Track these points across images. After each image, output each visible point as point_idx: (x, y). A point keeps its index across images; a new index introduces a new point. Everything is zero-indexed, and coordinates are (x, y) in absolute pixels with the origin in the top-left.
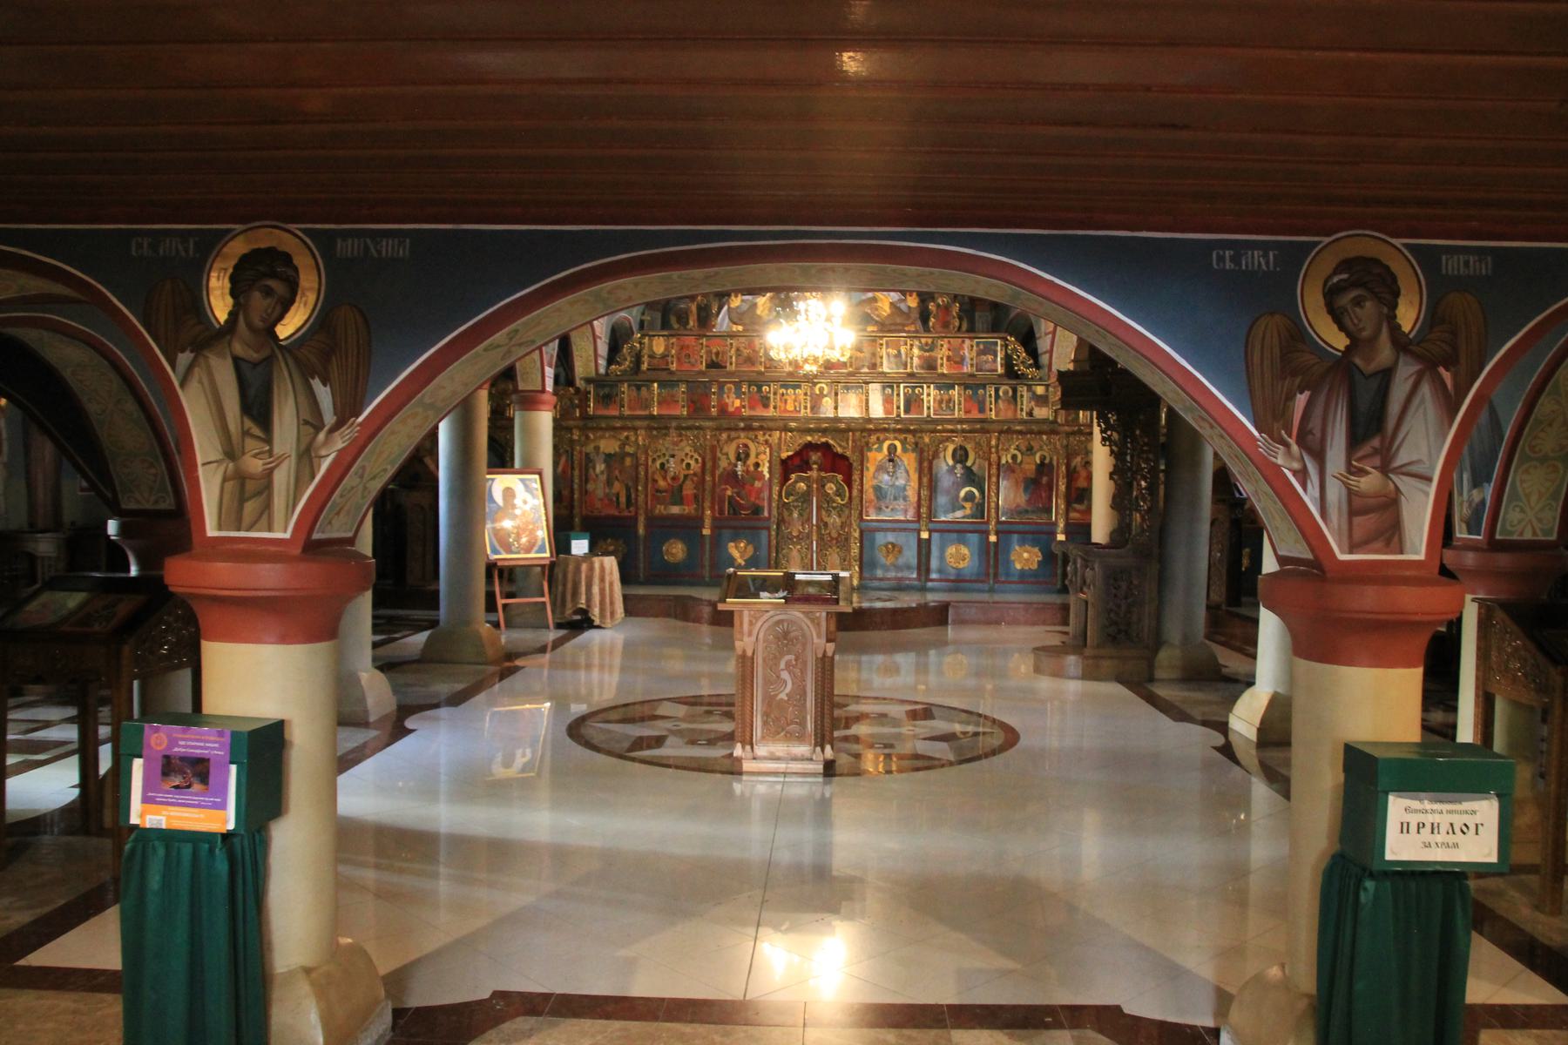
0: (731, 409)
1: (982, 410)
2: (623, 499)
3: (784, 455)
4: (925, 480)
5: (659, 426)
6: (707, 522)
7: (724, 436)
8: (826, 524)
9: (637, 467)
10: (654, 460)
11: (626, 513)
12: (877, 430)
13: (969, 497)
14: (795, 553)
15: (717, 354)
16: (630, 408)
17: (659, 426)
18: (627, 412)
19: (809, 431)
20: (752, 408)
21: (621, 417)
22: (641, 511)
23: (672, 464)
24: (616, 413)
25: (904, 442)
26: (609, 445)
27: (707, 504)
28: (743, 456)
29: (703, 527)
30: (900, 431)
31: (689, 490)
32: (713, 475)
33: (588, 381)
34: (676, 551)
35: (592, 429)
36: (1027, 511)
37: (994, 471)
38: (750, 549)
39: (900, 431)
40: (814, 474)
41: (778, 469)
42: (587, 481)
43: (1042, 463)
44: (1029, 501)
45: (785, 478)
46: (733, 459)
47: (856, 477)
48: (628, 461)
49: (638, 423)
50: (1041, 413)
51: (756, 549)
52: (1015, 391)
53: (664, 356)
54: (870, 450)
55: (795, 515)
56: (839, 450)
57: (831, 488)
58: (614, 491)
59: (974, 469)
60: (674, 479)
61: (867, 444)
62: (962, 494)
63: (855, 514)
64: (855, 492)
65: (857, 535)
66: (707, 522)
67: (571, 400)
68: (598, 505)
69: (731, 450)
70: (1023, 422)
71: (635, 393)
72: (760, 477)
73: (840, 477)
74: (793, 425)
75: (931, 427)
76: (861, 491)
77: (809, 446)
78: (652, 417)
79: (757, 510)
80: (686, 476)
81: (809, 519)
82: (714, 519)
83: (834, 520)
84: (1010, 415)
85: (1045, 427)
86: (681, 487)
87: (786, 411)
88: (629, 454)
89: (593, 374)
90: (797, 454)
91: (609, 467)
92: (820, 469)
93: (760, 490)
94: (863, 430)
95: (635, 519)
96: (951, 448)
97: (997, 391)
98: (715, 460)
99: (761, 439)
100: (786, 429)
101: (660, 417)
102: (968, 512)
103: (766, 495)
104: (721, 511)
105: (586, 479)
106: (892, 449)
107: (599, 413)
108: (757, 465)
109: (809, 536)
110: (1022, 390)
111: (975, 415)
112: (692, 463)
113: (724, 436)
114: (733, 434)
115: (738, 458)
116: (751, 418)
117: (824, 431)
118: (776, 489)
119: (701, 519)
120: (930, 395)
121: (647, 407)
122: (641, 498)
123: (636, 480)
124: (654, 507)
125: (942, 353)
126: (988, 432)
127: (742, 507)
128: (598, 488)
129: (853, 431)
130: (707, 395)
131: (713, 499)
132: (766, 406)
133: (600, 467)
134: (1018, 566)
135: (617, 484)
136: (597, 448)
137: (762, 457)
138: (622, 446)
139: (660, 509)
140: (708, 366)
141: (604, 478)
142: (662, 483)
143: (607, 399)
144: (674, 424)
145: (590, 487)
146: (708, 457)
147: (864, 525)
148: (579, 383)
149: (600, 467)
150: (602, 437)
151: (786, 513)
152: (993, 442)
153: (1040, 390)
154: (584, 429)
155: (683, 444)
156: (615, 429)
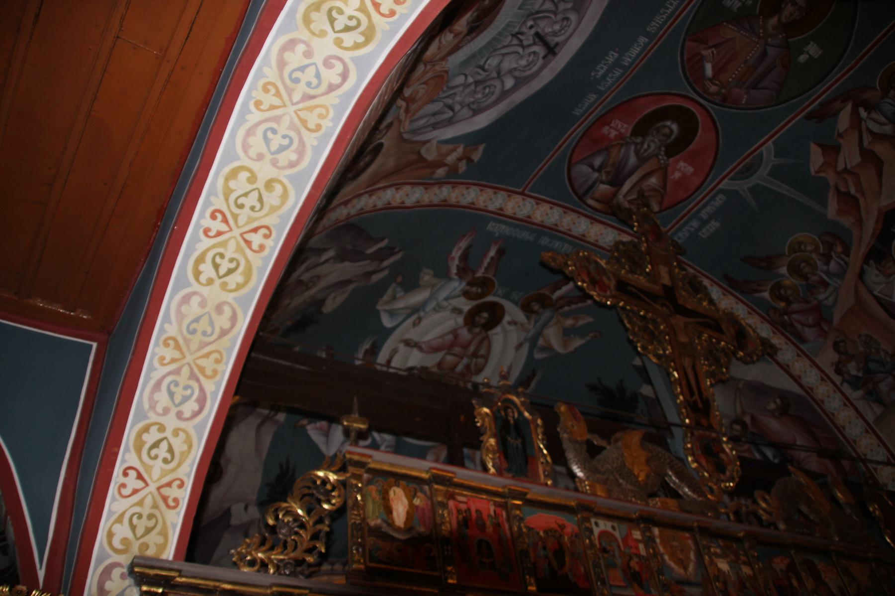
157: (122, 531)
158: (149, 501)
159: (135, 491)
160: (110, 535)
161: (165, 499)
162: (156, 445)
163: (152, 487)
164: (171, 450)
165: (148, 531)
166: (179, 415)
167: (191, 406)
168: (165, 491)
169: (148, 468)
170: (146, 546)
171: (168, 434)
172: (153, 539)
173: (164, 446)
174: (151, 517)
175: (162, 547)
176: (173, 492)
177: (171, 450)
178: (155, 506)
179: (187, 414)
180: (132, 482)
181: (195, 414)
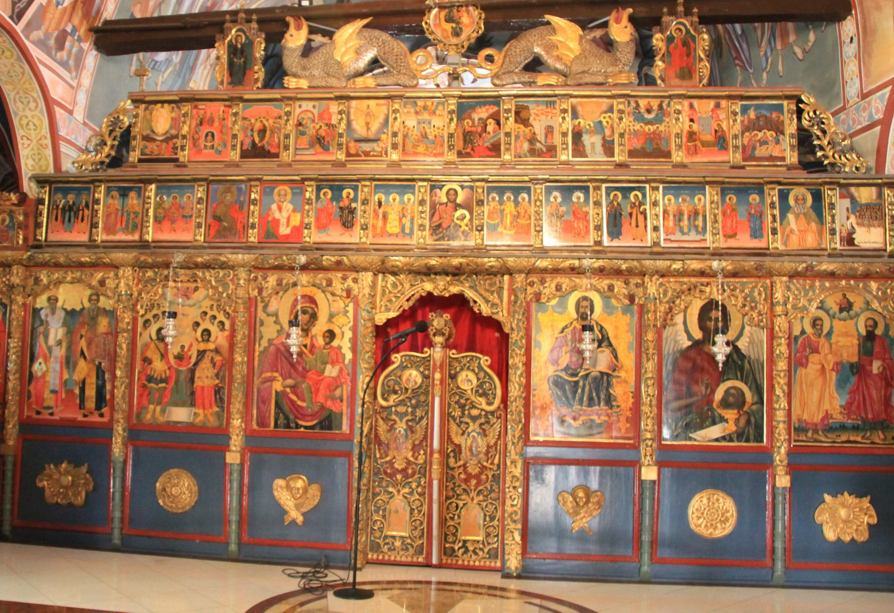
0: (284, 230)
1: (756, 233)
2: (91, 393)
3: (381, 318)
4: (650, 366)
5: (153, 260)
6: (236, 441)
7: (272, 280)
8: (458, 449)
9: (114, 333)
10: (147, 323)
11: (95, 418)
12: (556, 271)
13: (734, 401)
14: (398, 502)
15: (263, 132)
16: (108, 230)
17: (153, 260)
18: (101, 236)
19: (429, 272)
20: (321, 227)
21: (91, 245)
22: (119, 416)
23: (170, 327)
24: (84, 238)
25: (608, 294)
26: (71, 296)
27: (237, 406)
28: (305, 316)
29: (226, 448)
30: (601, 272)
31: (205, 377)
32: (250, 353)
33: (41, 181)
34: (179, 490)
35: (44, 265)
36: (843, 427)
37: (782, 348)
38: (315, 491)
39: (601, 272)
40: (437, 353)
41: (368, 345)
42: (32, 360)
43: (870, 336)
44: (847, 408)
45: (383, 363)
46: (284, 320)
47: (516, 360)
48: (103, 324)
49: (118, 256)
50: (869, 237)
51: (323, 492)
52: (817, 197)
53: (169, 138)
54: (543, 308)
55: (401, 427)
56: (486, 310)
57: (467, 380)
58: (77, 377)
59: (742, 344)
60: (179, 358)
61: (538, 297)
62: (719, 394)
63: (514, 431)
64: (515, 390)
65: (518, 471)
66: (236, 441)
67: (11, 214)
68: (49, 399)
69: (282, 306)
70: (834, 255)
71: (117, 203)
72: (336, 357)
73: (485, 361)
74: (398, 260)
75: (661, 264)
76: (527, 387)
77: (429, 302)
78: (143, 245)
79: (328, 422)
80: (201, 354)
81: (427, 436)
82: (249, 435)
83: (472, 441)
84: (811, 241)
85: (878, 266)
86: (192, 371)
87: (384, 233)
88: (105, 312)
89: (51, 170)
90: (407, 316)
91: (70, 333)
92: (447, 346)
93: (336, 383)
94: (530, 271)
95: (108, 429)
96: (697, 305)
97: (784, 196)
98: (253, 325)
99: (338, 286)
100: (384, 270)
101: (159, 245)
102: (731, 427)
103: (345, 391)
104: (262, 423)
105: (29, 355)
106: (584, 310)
107: (53, 237)
108: (331, 335)
109: (424, 470)
110: (831, 195)
111: (744, 240)
112: (214, 329)
113: (272, 280)
114: (289, 278)
115: (293, 323)
116: (320, 248)
117: (456, 273)
118: (363, 380)
119: (223, 433)
120: (659, 203)
121: (140, 226)
122: (119, 393)
123: (113, 358)
124: (142, 408)
125: (678, 123)
126: (770, 274)
127: (300, 413)
128: (49, 370)
129: (510, 272)
130: (241, 206)
131: (248, 395)
132: (348, 224)
133: (56, 331)
134: (830, 535)
135: (82, 363)
136: (53, 300)
137: (341, 320)
138: (95, 297)
139: (153, 414)
140: (245, 155)
141: (59, 352)
142: (159, 366)
143: (69, 214)
144: (179, 257)
145: (38, 368)
146: (241, 318)
147: (531, 451)
148: (30, 188)
149: (56, 331)
150: (59, 283)
151: (382, 427)
152: (778, 295)
153: (866, 195)
154: (31, 265)
155: (201, 294)
156: (81, 265)
157: (30, 162)
158: (35, 148)
159: (29, 145)
160: (26, 165)
161: (41, 145)
162: (28, 124)
163: (35, 142)
164: (35, 125)
165: (40, 160)
166: (30, 109)
167: (32, 105)
168: (41, 142)
169: (30, 135)
170: (41, 166)
171: (30, 118)
172: (43, 162)
173: (31, 124)
174: (39, 154)
175: (48, 166)
176: (44, 142)
177: (35, 125)
178: (39, 149)
179: (33, 108)
180: (27, 142)
181: (37, 107)
